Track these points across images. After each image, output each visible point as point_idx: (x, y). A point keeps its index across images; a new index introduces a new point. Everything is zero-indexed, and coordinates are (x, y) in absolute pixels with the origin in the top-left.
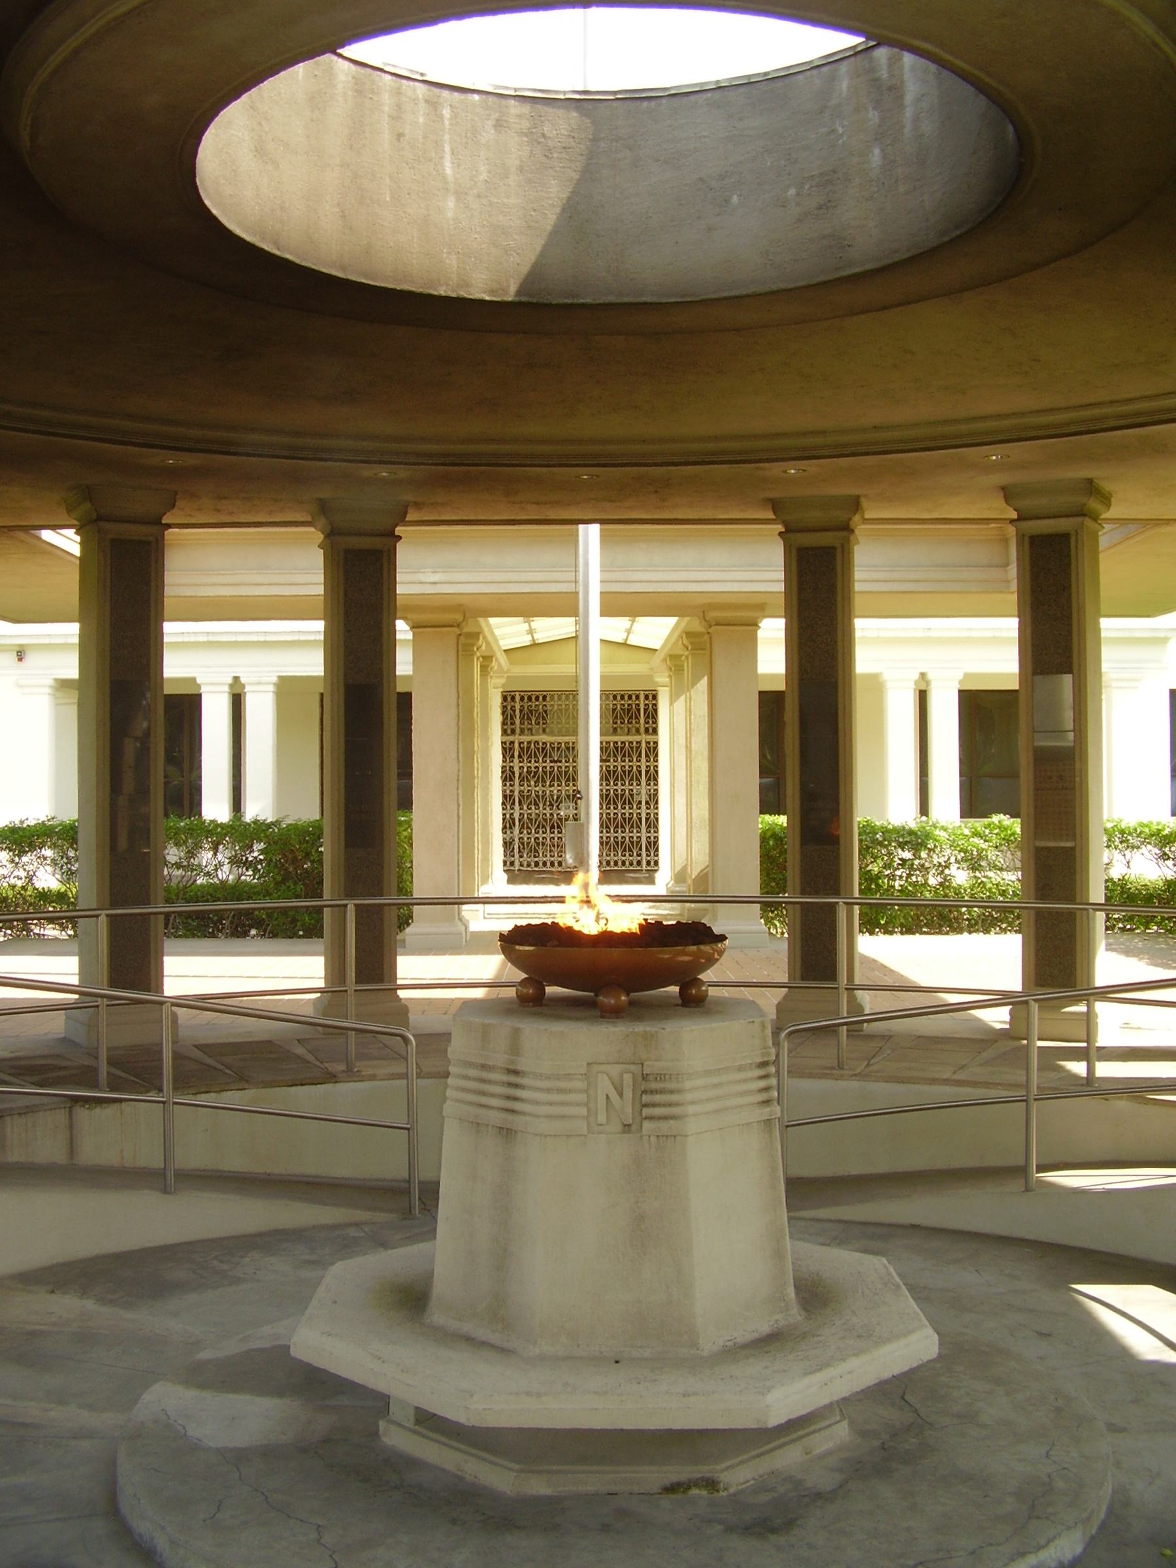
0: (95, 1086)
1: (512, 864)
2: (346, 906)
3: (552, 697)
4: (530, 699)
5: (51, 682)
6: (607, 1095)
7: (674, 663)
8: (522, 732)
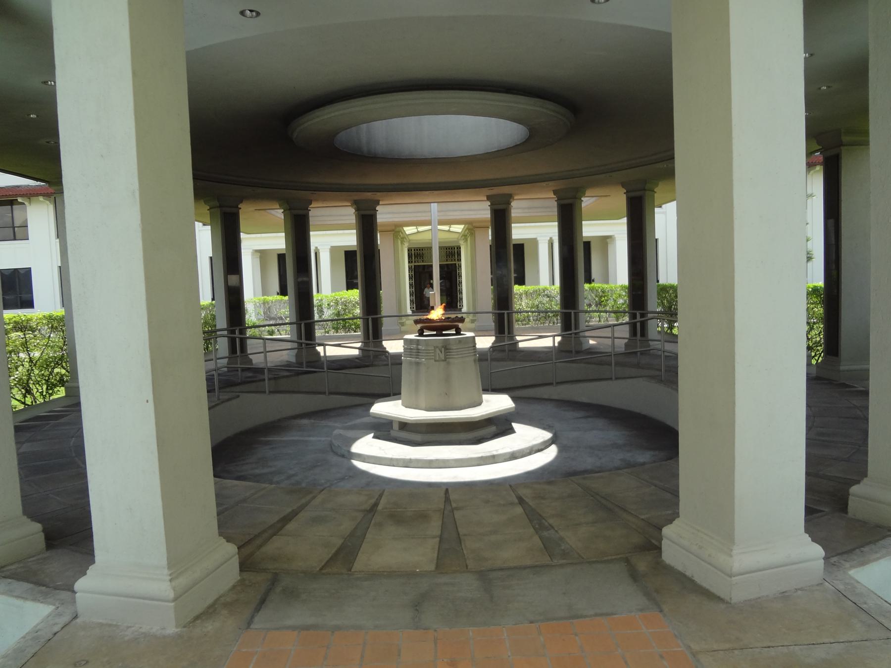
1: (413, 308)
3: (425, 249)
4: (417, 250)
5: (251, 251)
7: (464, 236)
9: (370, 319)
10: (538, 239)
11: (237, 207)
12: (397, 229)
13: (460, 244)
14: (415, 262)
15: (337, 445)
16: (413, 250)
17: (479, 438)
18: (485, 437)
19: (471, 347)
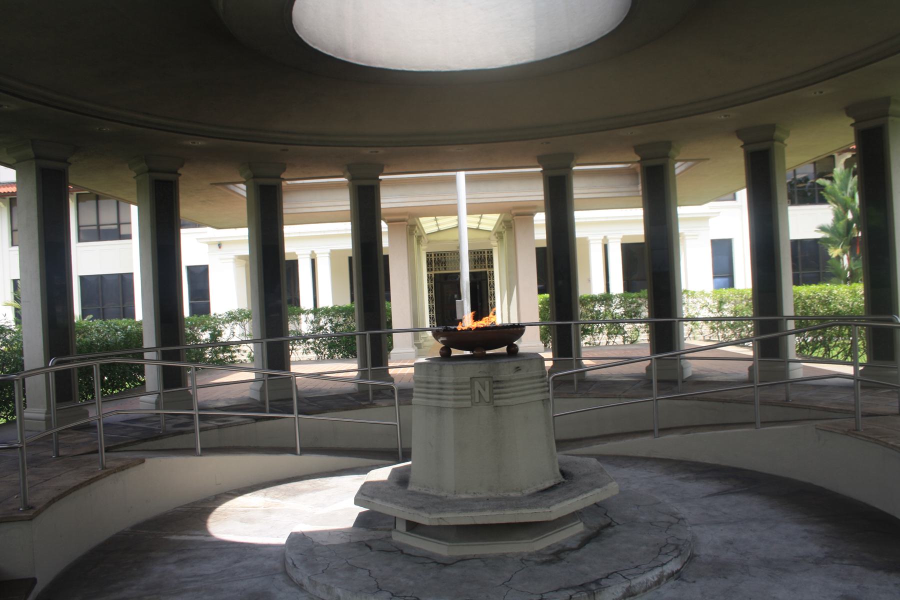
0: (265, 412)
3: (448, 254)
6: (479, 391)
7: (499, 235)
8: (435, 270)
9: (368, 334)
10: (590, 238)
11: (176, 172)
13: (492, 245)
15: (290, 561)
17: (557, 549)
18: (568, 546)
19: (536, 377)
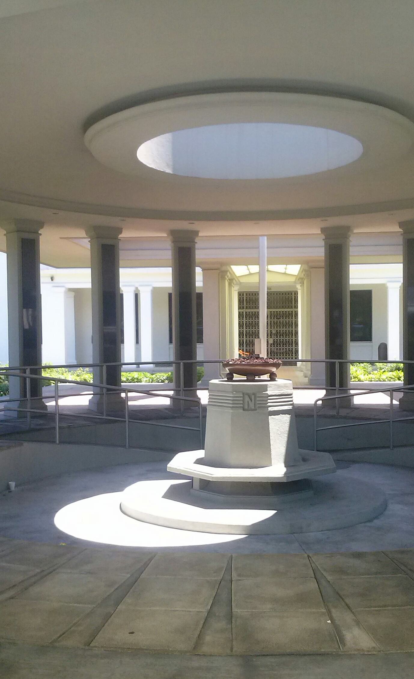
2: (180, 363)
4: (249, 295)
8: (247, 308)
9: (181, 363)
12: (224, 268)
13: (297, 289)
14: (247, 308)
16: (245, 295)
